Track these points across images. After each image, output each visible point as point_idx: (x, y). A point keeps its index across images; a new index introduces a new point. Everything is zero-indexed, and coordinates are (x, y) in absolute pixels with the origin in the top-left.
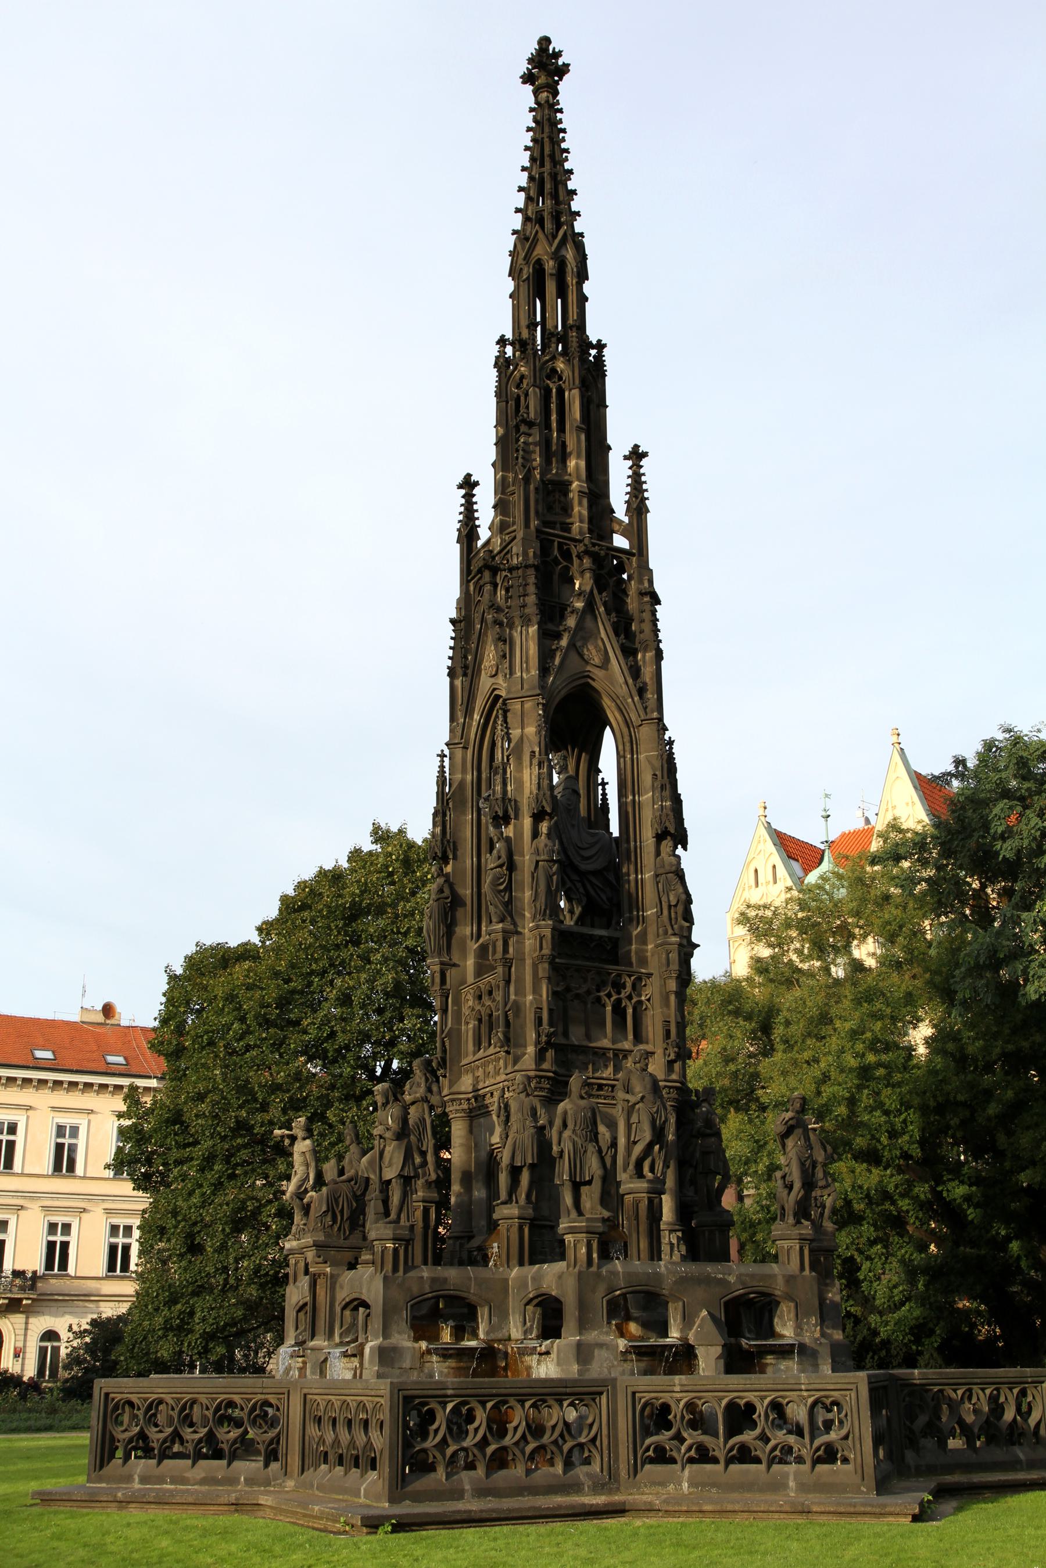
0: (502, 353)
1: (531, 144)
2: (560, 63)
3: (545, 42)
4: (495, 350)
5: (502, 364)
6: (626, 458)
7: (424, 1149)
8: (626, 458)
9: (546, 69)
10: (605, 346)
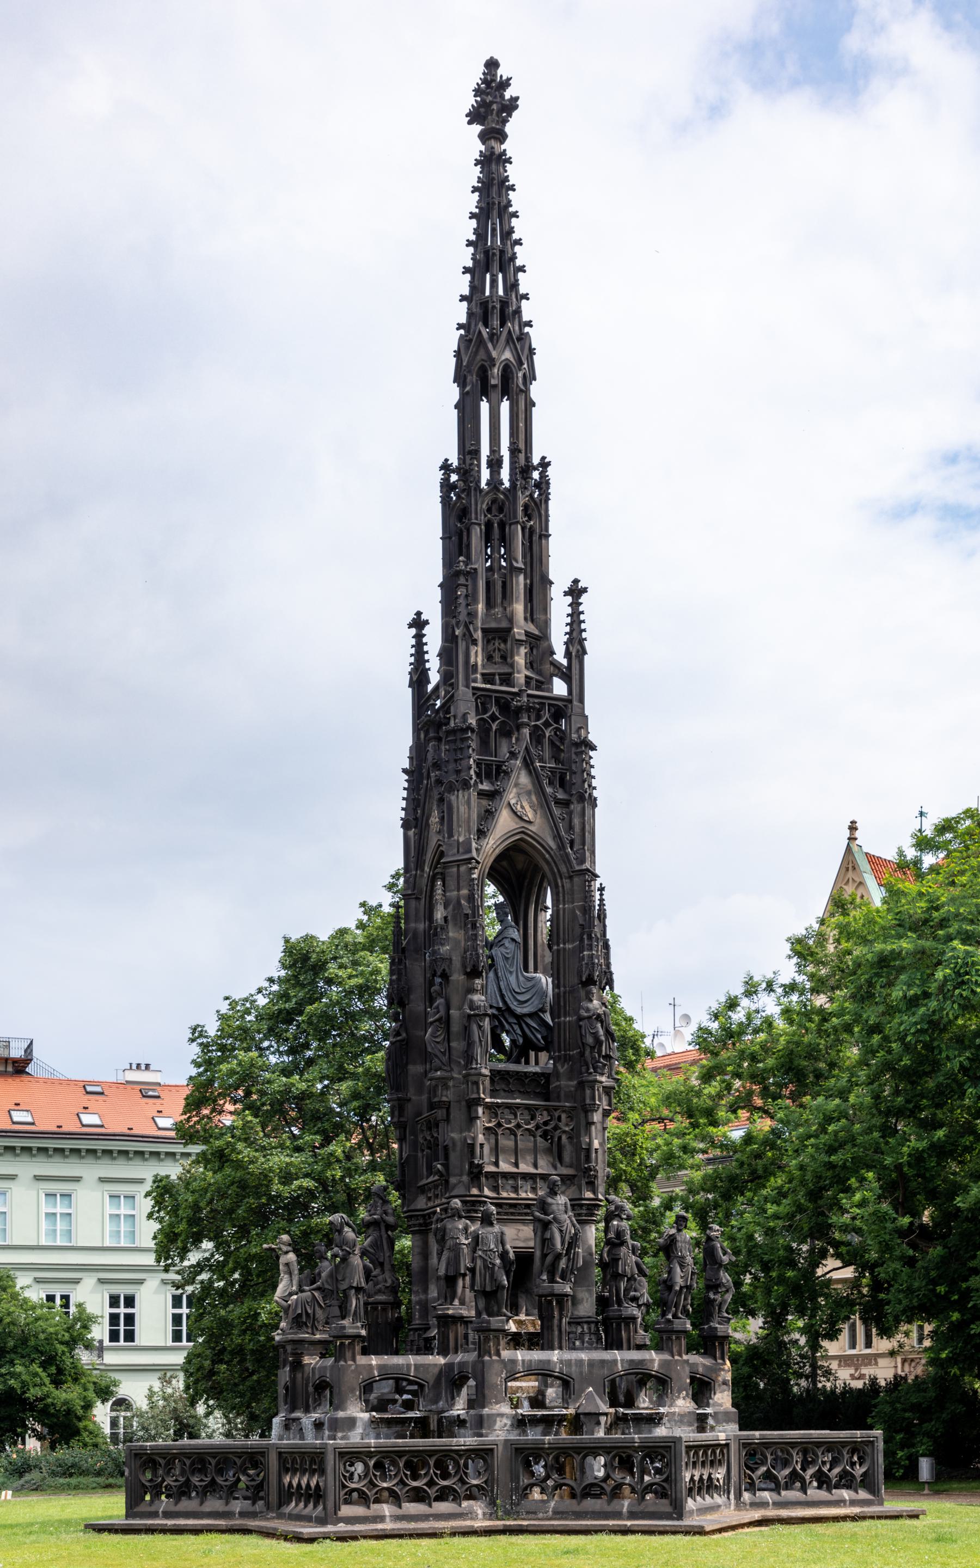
2: (507, 96)
3: (492, 64)
6: (566, 594)
7: (381, 1260)
8: (566, 594)
9: (492, 106)
10: (549, 464)
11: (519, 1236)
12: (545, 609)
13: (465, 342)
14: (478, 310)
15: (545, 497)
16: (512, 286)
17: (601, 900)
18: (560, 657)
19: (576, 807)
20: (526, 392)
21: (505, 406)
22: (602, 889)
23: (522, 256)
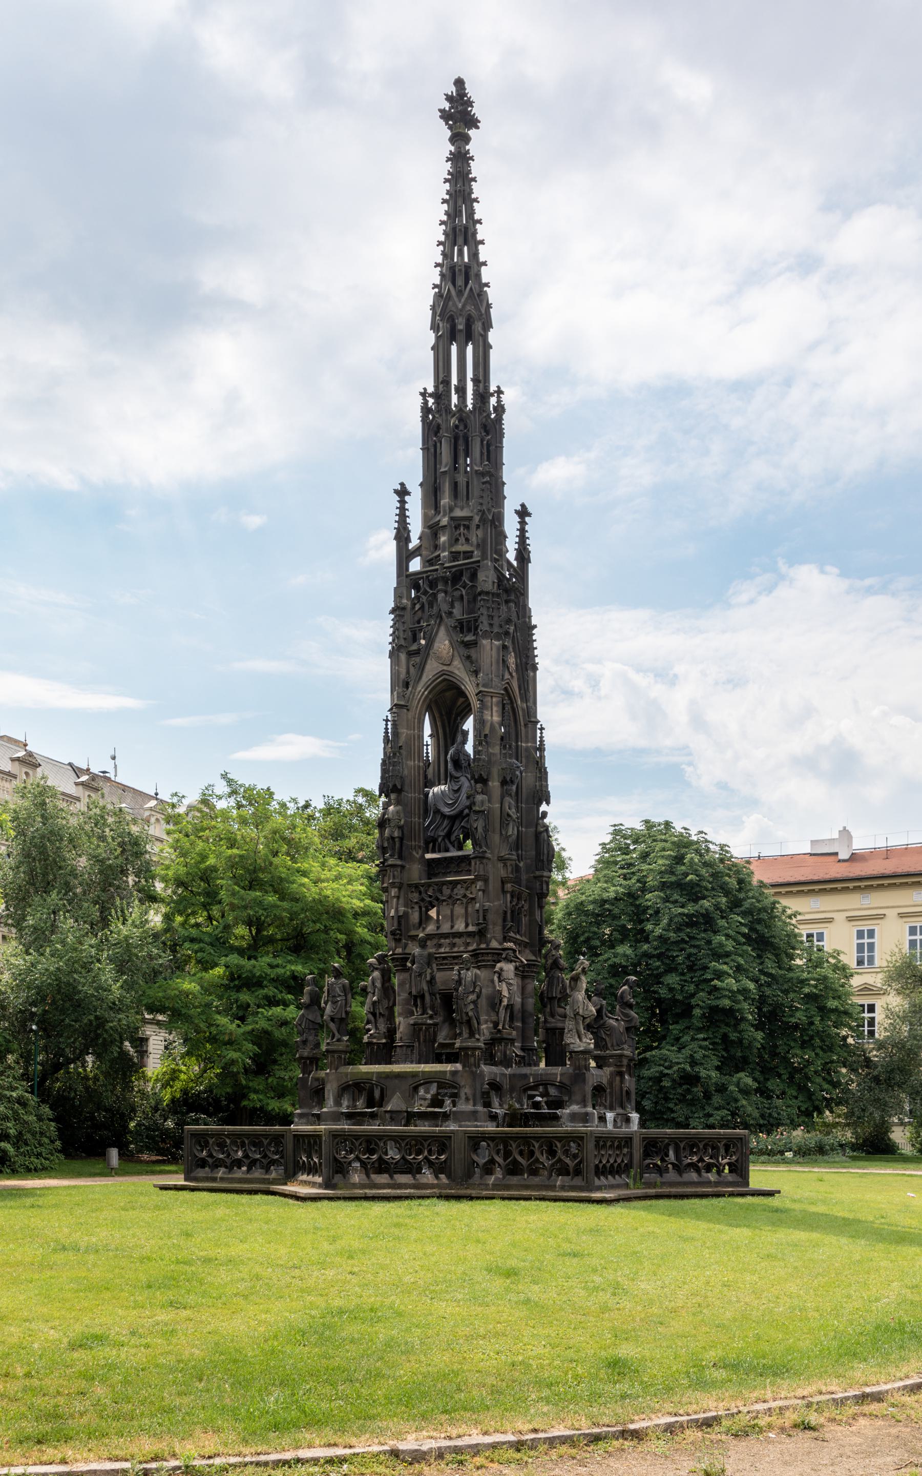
0: (426, 402)
1: (447, 197)
3: (459, 83)
4: (420, 399)
5: (426, 410)
9: (460, 115)
13: (438, 296)
14: (449, 275)
15: (499, 419)
16: (474, 255)
17: (541, 737)
20: (485, 338)
21: (470, 349)
22: (542, 729)
23: (482, 232)
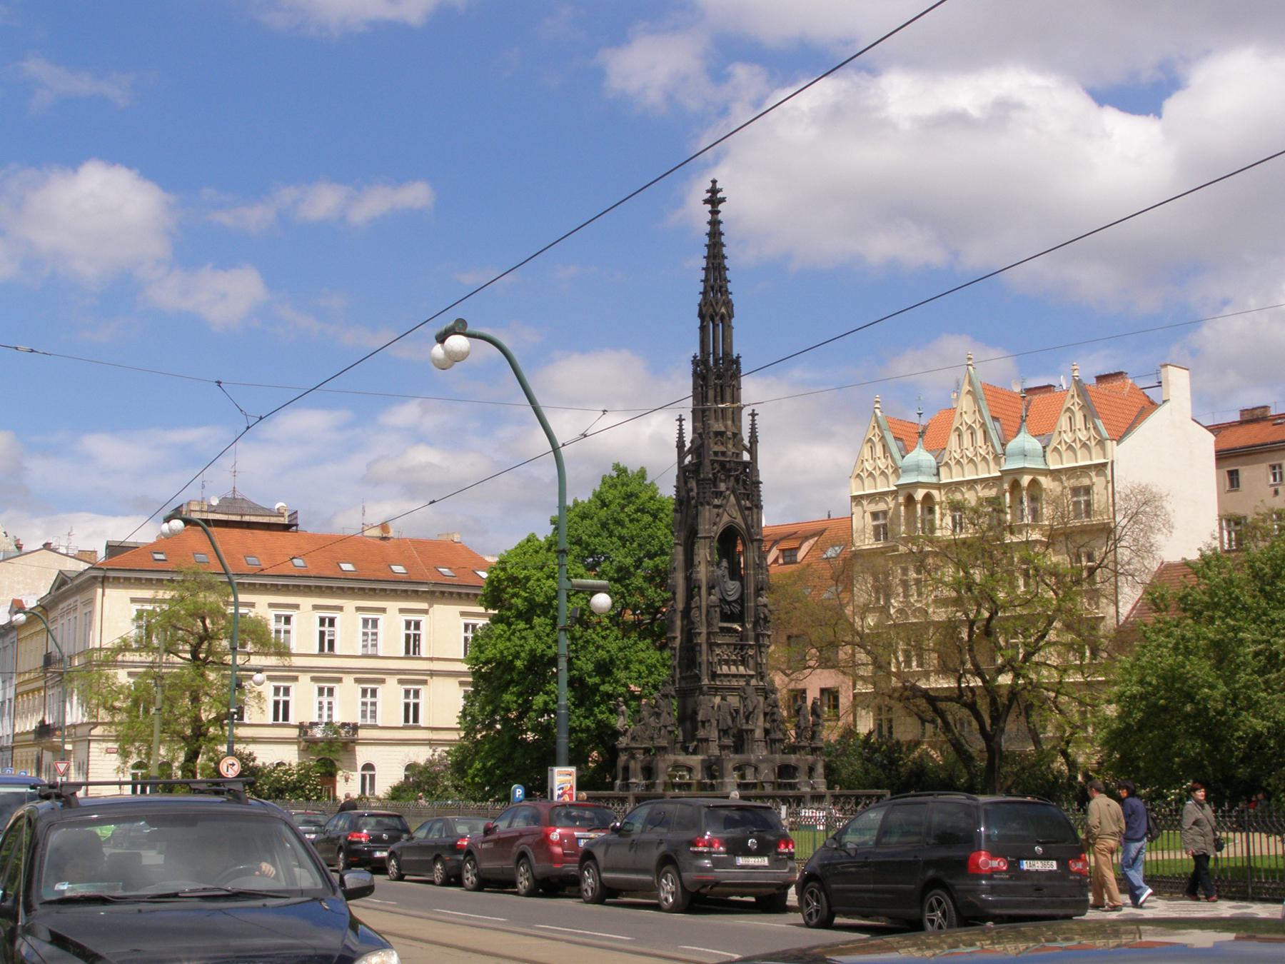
3: (714, 182)
11: (734, 700)
12: (740, 421)
18: (746, 442)
19: (755, 510)
